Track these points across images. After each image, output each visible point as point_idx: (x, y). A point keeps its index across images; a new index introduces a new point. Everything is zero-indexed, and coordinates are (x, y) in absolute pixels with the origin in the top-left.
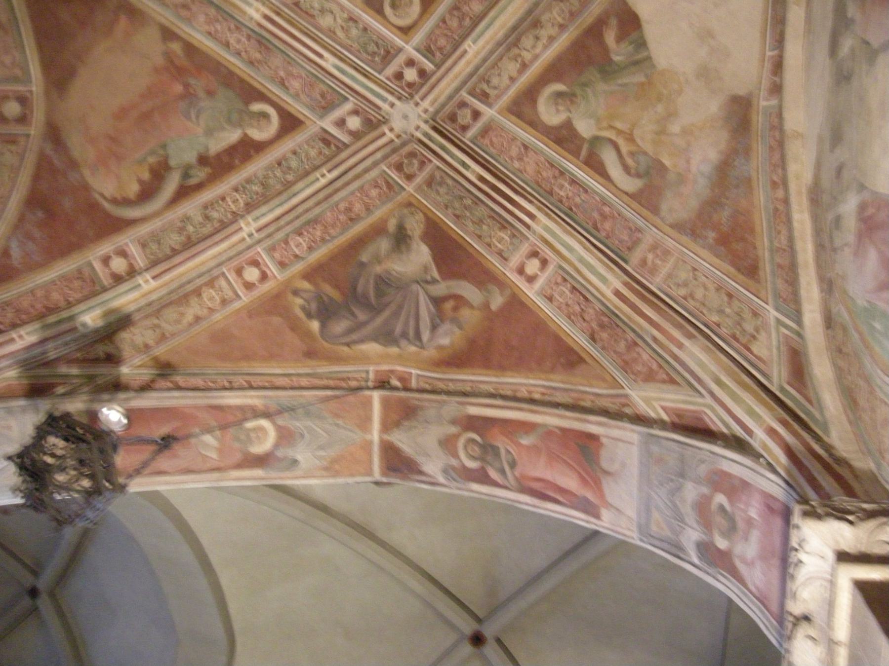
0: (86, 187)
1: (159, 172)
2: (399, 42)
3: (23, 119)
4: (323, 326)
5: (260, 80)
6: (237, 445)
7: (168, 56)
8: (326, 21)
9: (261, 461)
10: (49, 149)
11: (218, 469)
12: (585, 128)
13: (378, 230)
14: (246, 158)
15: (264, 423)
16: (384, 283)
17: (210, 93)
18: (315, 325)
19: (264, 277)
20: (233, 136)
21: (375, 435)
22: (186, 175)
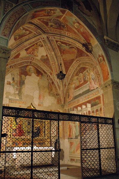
0: (77, 53)
1: (71, 48)
2: (42, 41)
3: (78, 60)
4: (65, 26)
5: (57, 47)
6: (80, 27)
7: (63, 55)
8: (48, 47)
9: (78, 23)
10: (78, 57)
11: (83, 27)
12: (24, 31)
13: (53, 28)
14: (63, 42)
15: (75, 26)
16: (56, 24)
17: (62, 49)
18: (65, 26)
19: (68, 33)
20: (63, 44)
21: (64, 15)
22: (69, 46)
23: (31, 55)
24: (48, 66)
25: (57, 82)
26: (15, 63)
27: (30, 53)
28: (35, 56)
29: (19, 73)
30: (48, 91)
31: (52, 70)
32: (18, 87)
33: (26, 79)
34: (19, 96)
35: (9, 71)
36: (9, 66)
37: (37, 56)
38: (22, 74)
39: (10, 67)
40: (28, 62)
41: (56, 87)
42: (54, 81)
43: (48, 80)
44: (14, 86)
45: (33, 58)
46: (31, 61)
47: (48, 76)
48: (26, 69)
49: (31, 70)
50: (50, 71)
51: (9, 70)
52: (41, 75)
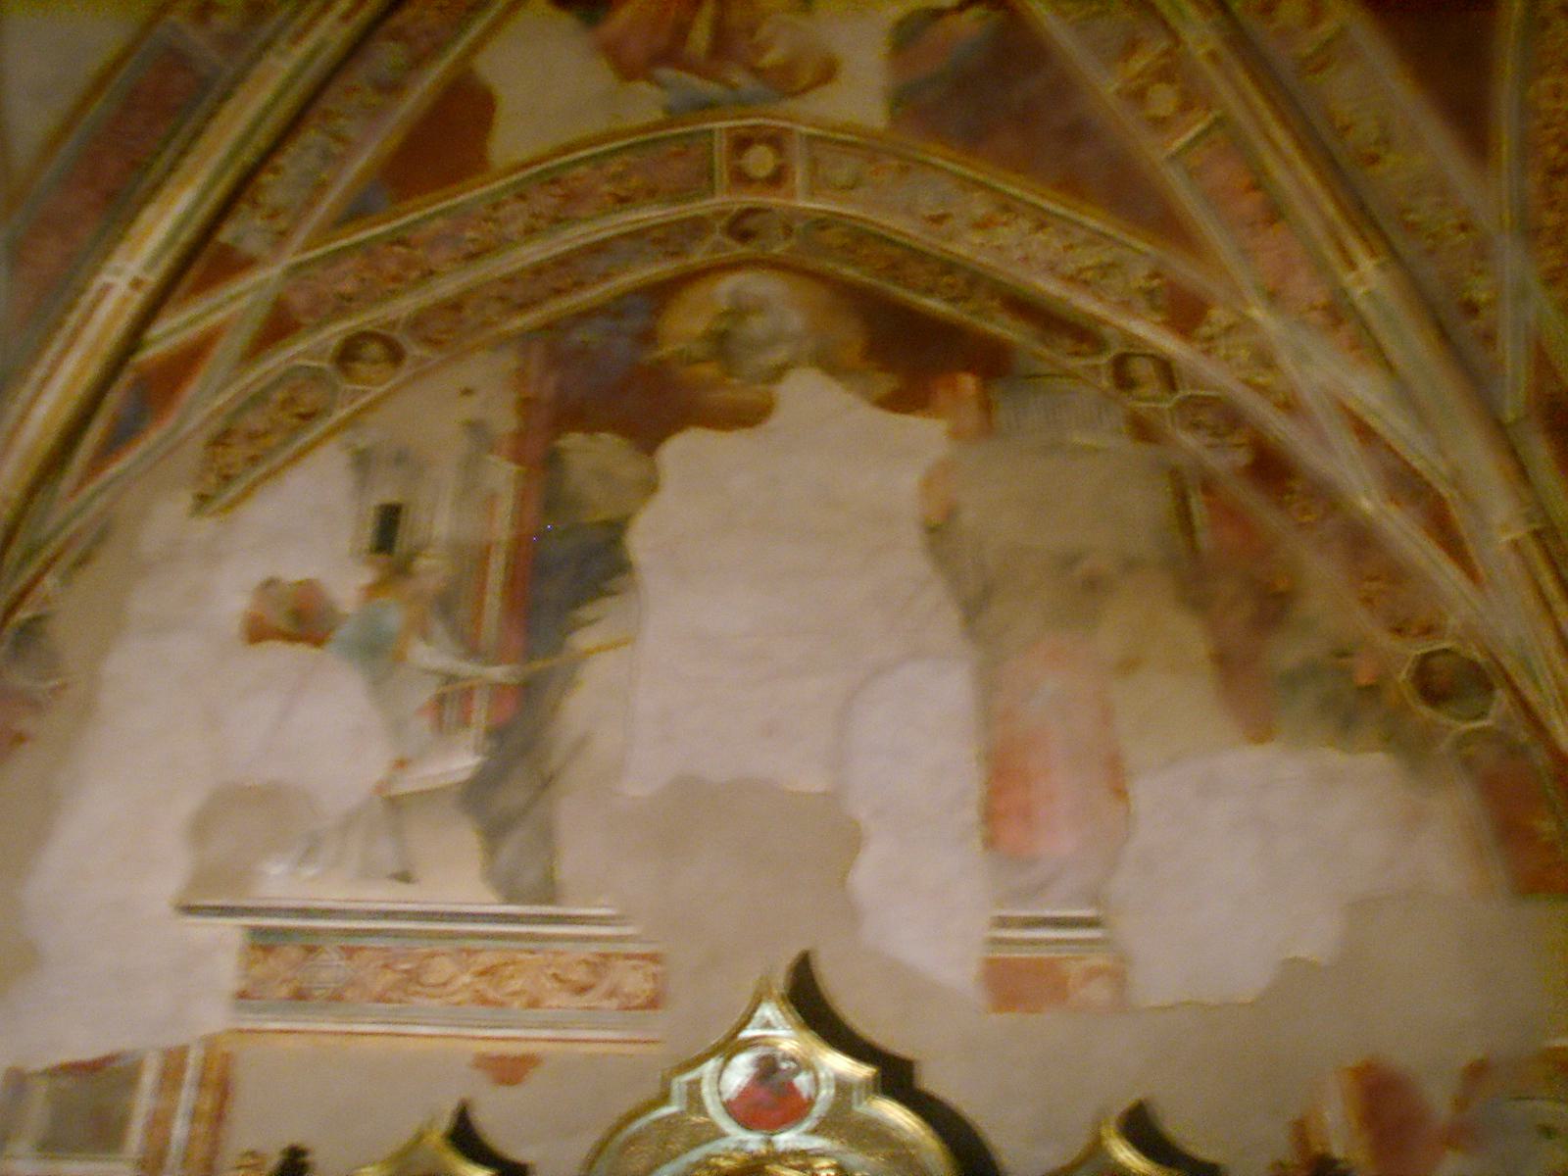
23: (712, 89)
24: (1071, 186)
25: (1364, 432)
26: (447, 287)
27: (671, 54)
28: (785, 82)
29: (504, 420)
30: (1190, 636)
31: (1170, 227)
32: (473, 650)
33: (650, 486)
34: (494, 832)
35: (307, 417)
36: (335, 333)
37: (828, 73)
38: (571, 415)
39: (348, 354)
40: (697, 227)
41: (1360, 540)
42: (1281, 428)
43: (1143, 430)
44: (400, 658)
45: (776, 141)
46: (750, 212)
47: (1141, 369)
48: (648, 337)
49: (757, 326)
50: (1142, 253)
51: (309, 399)
52: (968, 383)
